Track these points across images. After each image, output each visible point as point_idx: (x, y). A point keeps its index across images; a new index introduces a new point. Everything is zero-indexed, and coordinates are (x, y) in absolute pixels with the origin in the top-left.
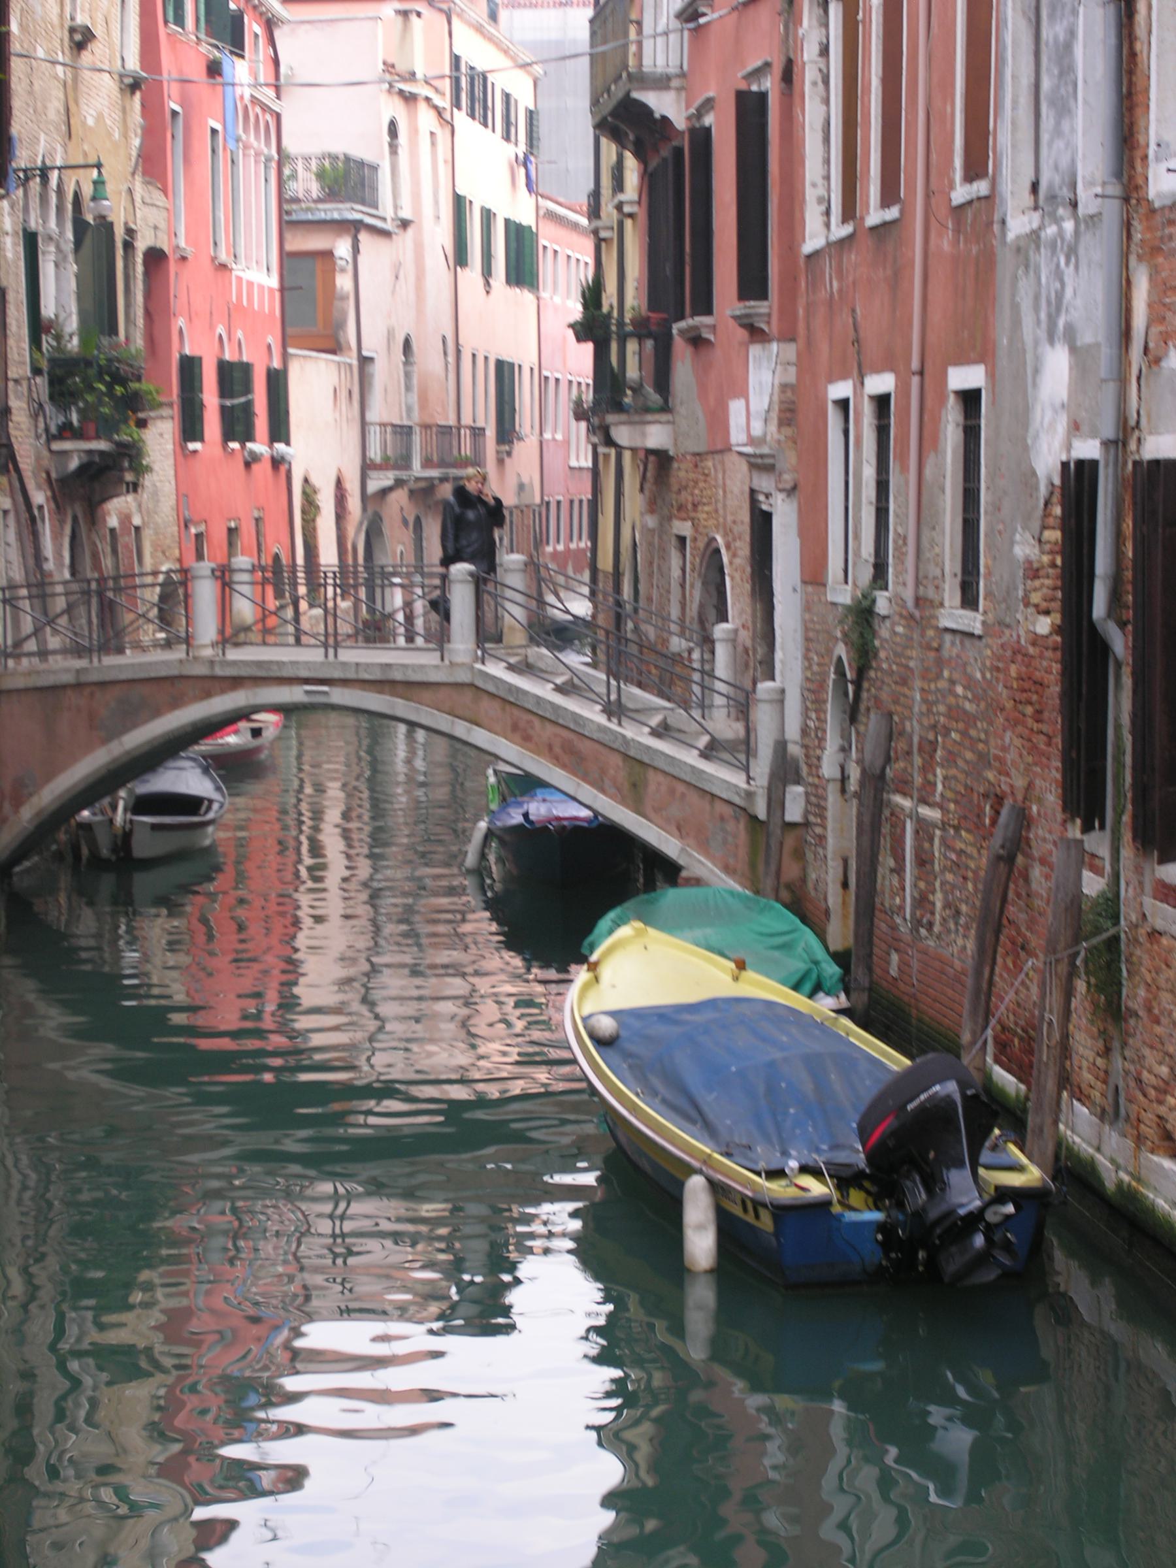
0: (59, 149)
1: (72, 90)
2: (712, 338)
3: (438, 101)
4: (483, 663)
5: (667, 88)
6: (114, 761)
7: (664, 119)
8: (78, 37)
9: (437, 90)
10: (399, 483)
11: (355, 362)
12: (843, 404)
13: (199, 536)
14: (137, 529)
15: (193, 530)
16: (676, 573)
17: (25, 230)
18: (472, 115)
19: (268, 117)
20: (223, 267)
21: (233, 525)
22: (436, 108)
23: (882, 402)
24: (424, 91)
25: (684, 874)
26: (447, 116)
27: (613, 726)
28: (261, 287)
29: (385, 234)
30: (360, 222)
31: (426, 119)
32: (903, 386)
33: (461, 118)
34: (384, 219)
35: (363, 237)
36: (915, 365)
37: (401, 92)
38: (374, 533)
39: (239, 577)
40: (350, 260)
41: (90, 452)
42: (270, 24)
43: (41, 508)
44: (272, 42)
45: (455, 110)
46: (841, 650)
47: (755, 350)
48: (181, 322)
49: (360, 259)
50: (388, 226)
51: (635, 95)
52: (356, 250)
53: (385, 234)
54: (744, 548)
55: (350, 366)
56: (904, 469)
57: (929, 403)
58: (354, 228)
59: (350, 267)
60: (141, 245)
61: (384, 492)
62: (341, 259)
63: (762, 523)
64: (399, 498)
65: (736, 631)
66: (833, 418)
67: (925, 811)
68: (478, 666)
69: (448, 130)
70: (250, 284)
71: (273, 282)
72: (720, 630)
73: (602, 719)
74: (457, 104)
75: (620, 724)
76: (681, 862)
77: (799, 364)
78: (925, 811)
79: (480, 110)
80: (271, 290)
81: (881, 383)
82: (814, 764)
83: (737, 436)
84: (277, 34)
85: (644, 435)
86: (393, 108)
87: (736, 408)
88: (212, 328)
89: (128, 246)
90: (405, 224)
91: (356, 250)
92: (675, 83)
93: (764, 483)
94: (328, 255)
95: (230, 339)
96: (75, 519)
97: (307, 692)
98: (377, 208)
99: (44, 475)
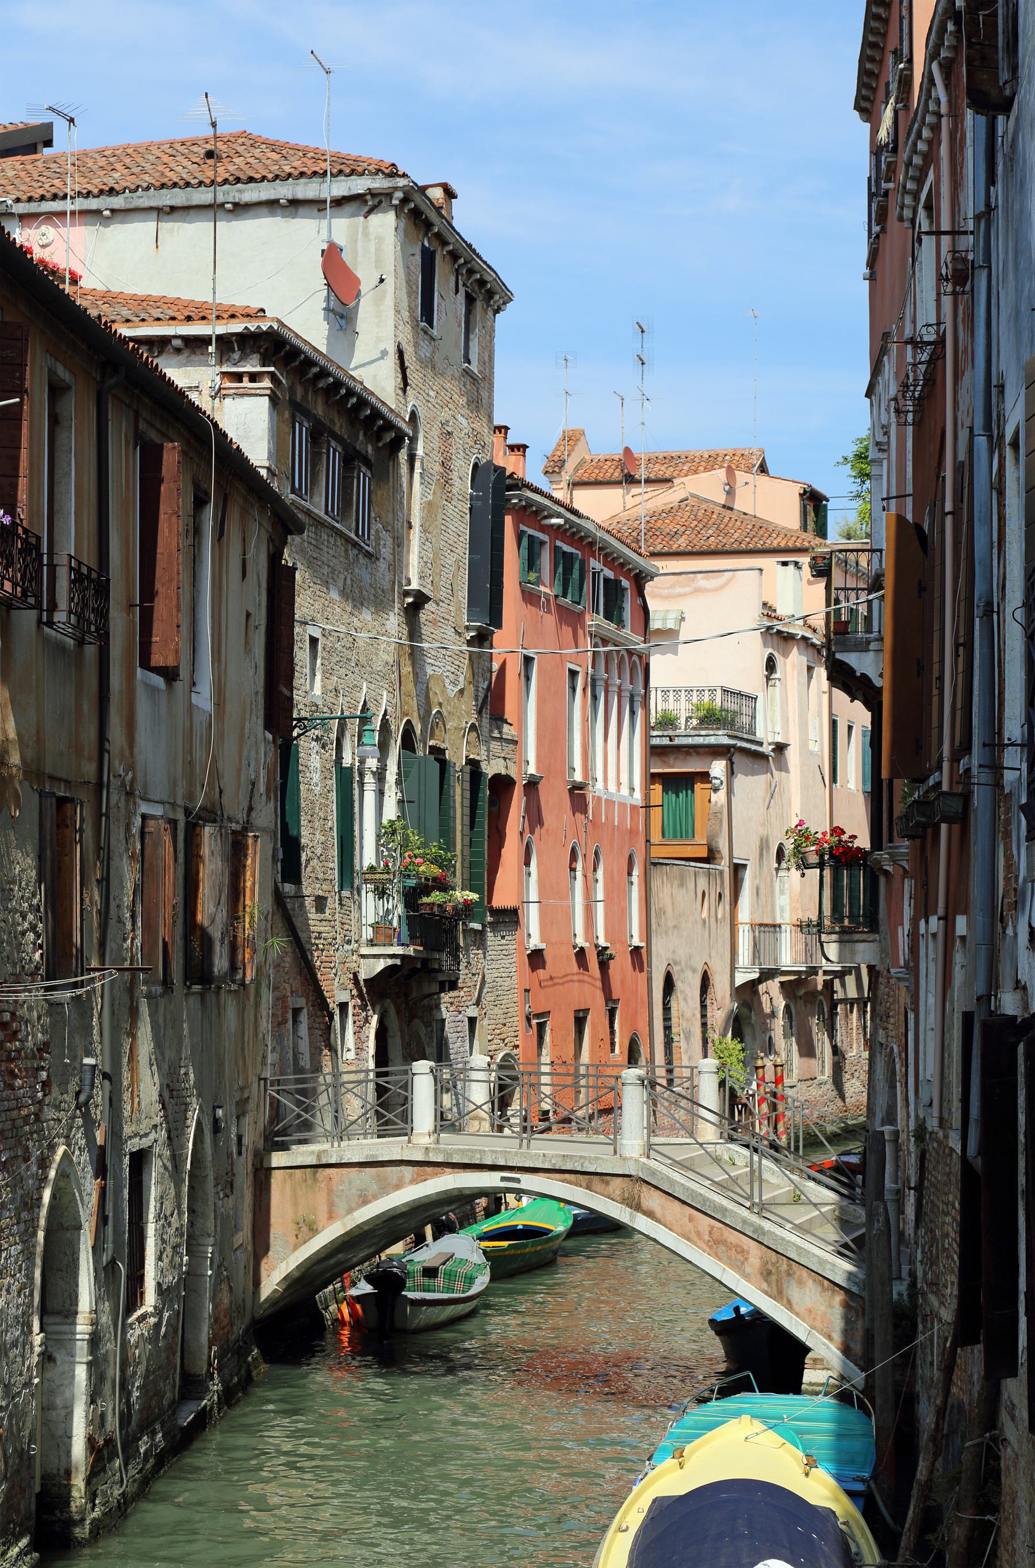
4: (648, 1157)
5: (867, 650)
7: (864, 676)
9: (815, 631)
10: (767, 975)
21: (581, 1015)
25: (810, 1355)
27: (754, 1218)
28: (622, 805)
30: (734, 746)
34: (761, 744)
37: (779, 632)
43: (343, 1007)
44: (640, 593)
50: (767, 749)
52: (731, 772)
62: (716, 778)
64: (773, 987)
76: (809, 1344)
80: (633, 808)
84: (649, 588)
90: (780, 748)
92: (873, 646)
99: (351, 976)
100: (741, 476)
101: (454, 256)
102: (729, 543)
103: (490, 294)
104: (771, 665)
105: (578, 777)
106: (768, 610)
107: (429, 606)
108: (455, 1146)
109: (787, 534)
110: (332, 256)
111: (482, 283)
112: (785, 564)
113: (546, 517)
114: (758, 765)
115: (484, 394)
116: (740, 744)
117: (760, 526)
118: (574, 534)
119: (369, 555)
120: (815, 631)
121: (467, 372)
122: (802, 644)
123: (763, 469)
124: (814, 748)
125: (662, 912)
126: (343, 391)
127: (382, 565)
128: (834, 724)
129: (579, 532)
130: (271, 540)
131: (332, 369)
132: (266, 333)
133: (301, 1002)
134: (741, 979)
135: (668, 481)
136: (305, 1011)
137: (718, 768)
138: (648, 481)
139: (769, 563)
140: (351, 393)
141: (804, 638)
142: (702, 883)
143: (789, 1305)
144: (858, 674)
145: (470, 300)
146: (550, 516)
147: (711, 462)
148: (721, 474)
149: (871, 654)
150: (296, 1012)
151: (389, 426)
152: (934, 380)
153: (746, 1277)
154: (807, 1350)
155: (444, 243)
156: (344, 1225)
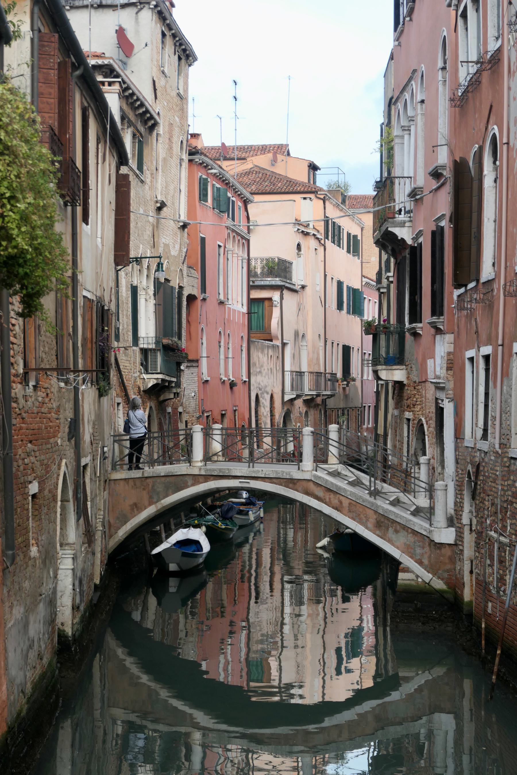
0: (149, 251)
1: (156, 227)
2: (421, 332)
3: (319, 236)
4: (316, 471)
5: (404, 226)
6: (158, 511)
7: (402, 239)
8: (159, 205)
9: (318, 231)
10: (298, 397)
11: (280, 345)
12: (471, 359)
13: (208, 417)
14: (180, 413)
15: (206, 415)
16: (406, 434)
17: (132, 285)
18: (333, 242)
19: (244, 241)
20: (221, 303)
21: (224, 412)
22: (318, 238)
23: (487, 358)
24: (312, 232)
25: (402, 566)
26: (322, 242)
27: (372, 499)
28: (239, 312)
29: (295, 291)
30: (284, 286)
31: (312, 243)
32: (495, 351)
33: (329, 244)
34: (294, 285)
35: (285, 292)
36: (500, 342)
37: (303, 232)
38: (287, 417)
39: (215, 432)
40: (279, 301)
41: (157, 379)
42: (246, 202)
44: (246, 210)
45: (326, 240)
46: (470, 467)
47: (438, 337)
48: (202, 326)
49: (283, 301)
50: (297, 288)
51: (390, 229)
52: (282, 298)
53: (295, 291)
54: (433, 423)
55: (278, 346)
56: (495, 386)
57: (506, 359)
58: (280, 288)
59: (279, 305)
60: (186, 293)
61: (292, 400)
63: (440, 412)
64: (299, 403)
65: (429, 460)
66: (468, 365)
67: (502, 539)
68: (314, 472)
69: (323, 248)
70: (234, 311)
71: (245, 310)
72: (423, 459)
73: (367, 497)
74: (327, 237)
75: (375, 499)
76: (400, 560)
77: (455, 343)
78: (502, 539)
79: (337, 240)
80: (243, 313)
81: (487, 350)
82: (459, 519)
83: (430, 375)
84: (249, 206)
85: (393, 375)
86: (299, 239)
87: (430, 363)
88: (216, 329)
89: (180, 294)
90: (303, 287)
91: (282, 298)
92: (407, 224)
93: (441, 395)
94: (270, 299)
95: (224, 334)
96: (151, 408)
97: (240, 482)
98: (291, 280)
100: (280, 157)
101: (174, 36)
102: (276, 189)
103: (188, 57)
104: (299, 247)
105: (222, 297)
106: (298, 222)
107: (165, 209)
108: (213, 467)
109: (302, 184)
110: (121, 32)
111: (184, 50)
112: (305, 198)
113: (209, 169)
114: (295, 294)
115: (185, 106)
116: (287, 285)
117: (290, 182)
118: (220, 178)
119: (142, 182)
120: (318, 231)
121: (179, 95)
122: (313, 237)
123: (289, 154)
124: (318, 288)
125: (255, 364)
126: (135, 98)
127: (147, 187)
128: (325, 276)
129: (223, 177)
130: (117, 167)
131: (132, 86)
132: (107, 65)
133: (119, 400)
134: (287, 398)
135: (244, 159)
136: (121, 405)
137: (276, 296)
138: (238, 159)
139: (298, 197)
140: (138, 99)
141: (314, 235)
142: (271, 352)
143: (390, 541)
144: (399, 238)
145: (180, 59)
146: (211, 169)
147: (263, 149)
148: (270, 156)
149: (406, 229)
150: (118, 404)
151: (152, 118)
152: (480, 82)
153: (367, 528)
154: (400, 563)
155: (170, 29)
156: (156, 507)
